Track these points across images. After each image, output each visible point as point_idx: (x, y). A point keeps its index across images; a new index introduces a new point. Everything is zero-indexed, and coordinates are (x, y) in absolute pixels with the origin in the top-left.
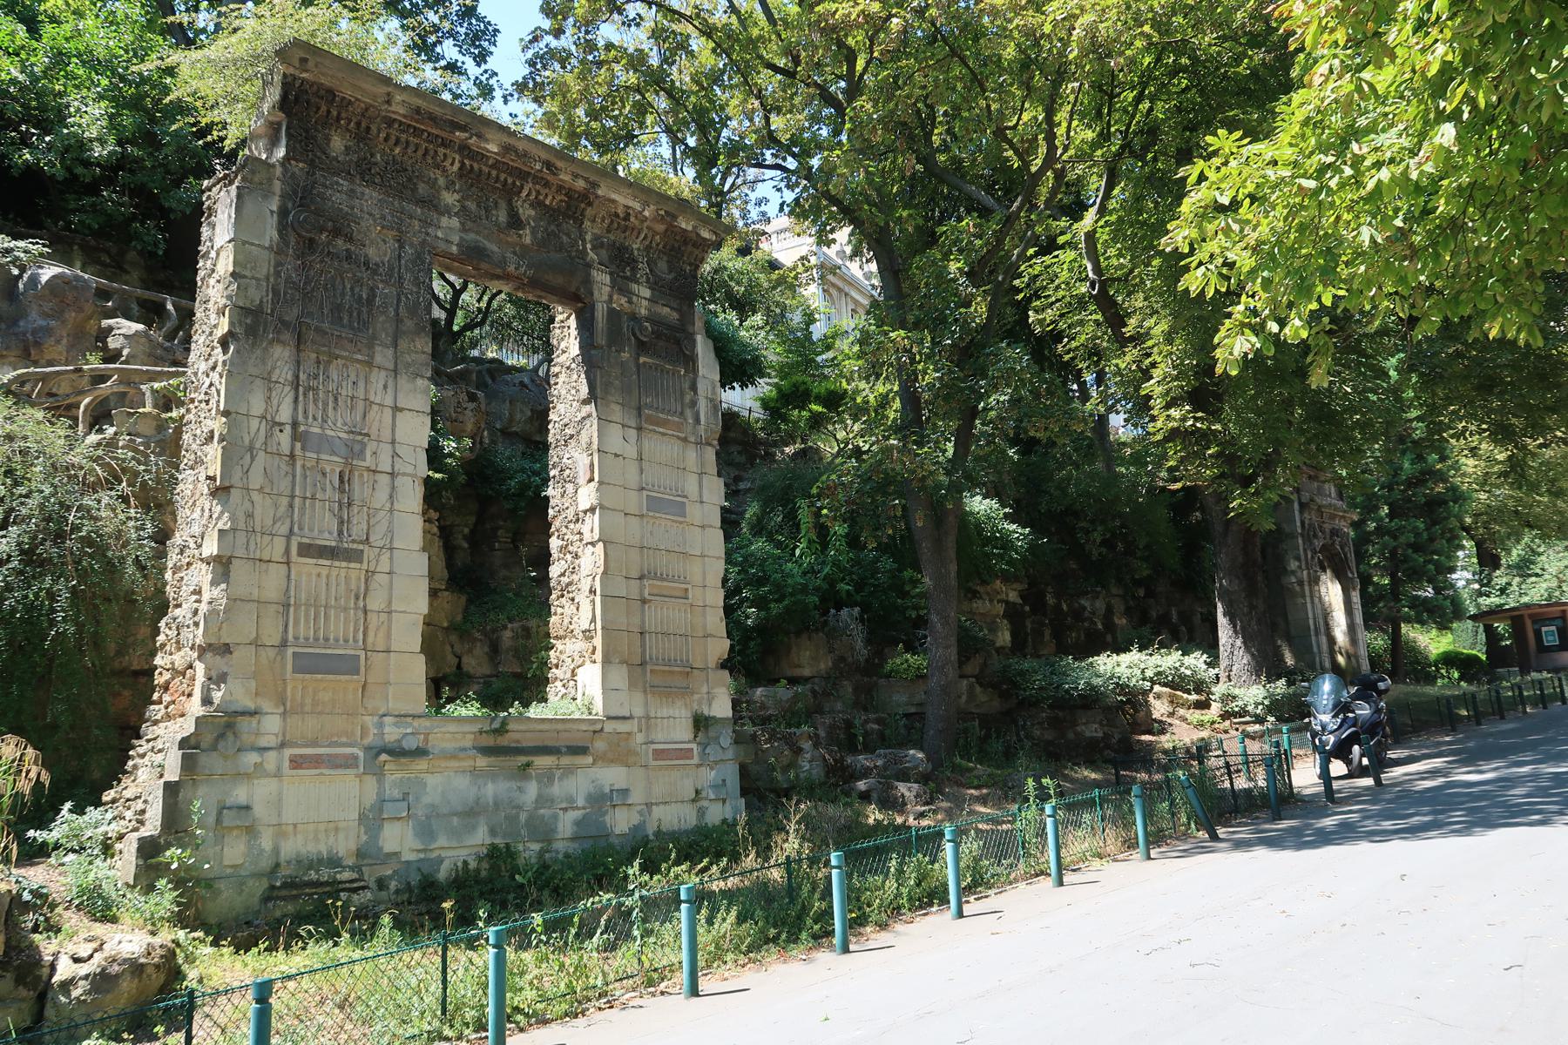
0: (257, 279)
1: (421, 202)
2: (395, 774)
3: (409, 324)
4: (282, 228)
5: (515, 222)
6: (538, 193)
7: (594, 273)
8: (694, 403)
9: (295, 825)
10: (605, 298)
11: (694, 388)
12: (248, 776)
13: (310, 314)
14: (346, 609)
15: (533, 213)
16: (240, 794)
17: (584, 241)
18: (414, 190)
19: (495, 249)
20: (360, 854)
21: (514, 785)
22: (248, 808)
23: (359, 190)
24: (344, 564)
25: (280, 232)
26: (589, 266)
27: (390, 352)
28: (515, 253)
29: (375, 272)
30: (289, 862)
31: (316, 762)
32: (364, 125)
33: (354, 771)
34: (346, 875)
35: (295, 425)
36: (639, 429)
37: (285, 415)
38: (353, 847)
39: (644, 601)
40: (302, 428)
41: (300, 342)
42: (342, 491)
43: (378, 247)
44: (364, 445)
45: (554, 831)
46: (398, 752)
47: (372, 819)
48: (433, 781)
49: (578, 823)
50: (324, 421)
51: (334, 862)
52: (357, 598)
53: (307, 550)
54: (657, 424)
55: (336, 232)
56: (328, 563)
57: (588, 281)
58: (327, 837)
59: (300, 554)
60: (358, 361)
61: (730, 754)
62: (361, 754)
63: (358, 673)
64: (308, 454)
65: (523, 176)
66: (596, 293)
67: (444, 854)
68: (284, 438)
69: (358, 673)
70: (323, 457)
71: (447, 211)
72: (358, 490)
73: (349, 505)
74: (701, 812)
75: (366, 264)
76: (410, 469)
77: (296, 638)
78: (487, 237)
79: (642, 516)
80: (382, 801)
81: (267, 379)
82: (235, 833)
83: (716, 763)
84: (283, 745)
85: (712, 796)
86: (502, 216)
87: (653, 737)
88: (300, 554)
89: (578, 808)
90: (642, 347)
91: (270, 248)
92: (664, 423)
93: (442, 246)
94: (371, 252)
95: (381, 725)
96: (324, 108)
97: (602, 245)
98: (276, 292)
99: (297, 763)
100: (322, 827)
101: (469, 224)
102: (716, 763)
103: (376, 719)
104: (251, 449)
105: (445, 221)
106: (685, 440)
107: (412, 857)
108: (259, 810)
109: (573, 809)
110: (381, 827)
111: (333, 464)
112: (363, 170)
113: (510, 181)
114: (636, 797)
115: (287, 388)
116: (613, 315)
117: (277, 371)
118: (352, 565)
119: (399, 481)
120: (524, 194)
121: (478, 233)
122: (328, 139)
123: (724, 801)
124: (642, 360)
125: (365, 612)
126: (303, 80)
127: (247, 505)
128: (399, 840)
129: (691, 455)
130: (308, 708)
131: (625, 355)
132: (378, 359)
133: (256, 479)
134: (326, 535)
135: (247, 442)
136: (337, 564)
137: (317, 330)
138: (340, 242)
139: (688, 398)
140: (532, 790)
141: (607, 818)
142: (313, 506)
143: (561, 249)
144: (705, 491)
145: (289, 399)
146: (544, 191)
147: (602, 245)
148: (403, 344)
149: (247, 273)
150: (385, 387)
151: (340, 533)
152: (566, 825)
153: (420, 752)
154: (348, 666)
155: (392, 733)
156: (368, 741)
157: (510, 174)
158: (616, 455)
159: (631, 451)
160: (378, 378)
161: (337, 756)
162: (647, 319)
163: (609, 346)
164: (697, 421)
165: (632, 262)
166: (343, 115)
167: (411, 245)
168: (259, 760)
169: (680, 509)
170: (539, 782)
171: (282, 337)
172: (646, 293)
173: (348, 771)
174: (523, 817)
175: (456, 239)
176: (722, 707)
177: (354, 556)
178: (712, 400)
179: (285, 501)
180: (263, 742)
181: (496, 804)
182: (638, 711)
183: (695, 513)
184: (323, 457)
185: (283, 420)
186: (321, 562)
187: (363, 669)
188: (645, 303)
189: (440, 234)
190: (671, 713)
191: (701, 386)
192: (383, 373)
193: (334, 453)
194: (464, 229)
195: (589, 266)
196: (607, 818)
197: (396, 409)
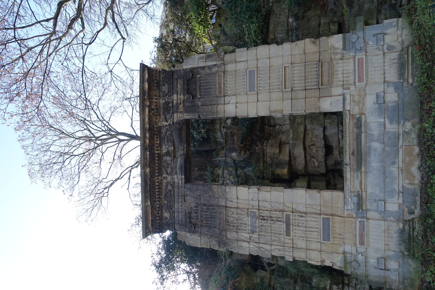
0: (210, 241)
1: (173, 187)
2: (368, 205)
3: (210, 193)
4: (194, 232)
5: (168, 154)
6: (157, 147)
7: (175, 121)
8: (209, 67)
9: (385, 245)
10: (182, 115)
11: (203, 68)
12: (366, 258)
13: (215, 227)
14: (307, 221)
15: (163, 146)
16: (372, 261)
17: (166, 126)
18: (170, 191)
19: (179, 160)
20: (398, 221)
21: (372, 154)
22: (378, 259)
23: (176, 210)
24: (291, 221)
25: (195, 233)
26: (173, 123)
27: (221, 200)
28: (178, 151)
29: (198, 204)
30: (399, 248)
31: (362, 236)
32: (158, 209)
33: (366, 222)
34: (407, 228)
35: (249, 233)
36: (224, 96)
37: (247, 235)
38: (395, 224)
39: (292, 90)
40: (250, 232)
41: (226, 230)
42: (267, 220)
43: (191, 202)
44: (251, 212)
45: (394, 133)
46: (360, 205)
47: (385, 215)
48: (369, 190)
49: (391, 122)
50: (246, 224)
51: (402, 232)
52: (302, 216)
53: (288, 234)
54: (221, 88)
55: (190, 218)
56: (291, 226)
57: (179, 123)
58: (391, 233)
59: (290, 236)
60: (226, 212)
61: (360, 34)
62: (359, 219)
63: (329, 219)
64: (257, 230)
65: (152, 155)
66: (181, 119)
67: (401, 185)
68: (255, 236)
69: (329, 219)
70: (257, 226)
71: (173, 179)
72: (266, 214)
73: (271, 217)
74: (390, 48)
75: (196, 207)
76: (256, 195)
77: (318, 239)
78: (176, 164)
79: (258, 93)
80: (377, 210)
81: (238, 240)
82: (386, 264)
83: (365, 42)
84: (355, 245)
85: (382, 43)
86: (168, 158)
87: (352, 82)
88: (290, 236)
89: (385, 121)
90: (194, 97)
91: (200, 236)
92: (220, 84)
93: (183, 181)
94: (193, 205)
95: (348, 210)
96: (158, 221)
97: (165, 118)
98: (212, 236)
99: (362, 243)
100: (386, 235)
101: (174, 171)
102: (365, 42)
103: (345, 211)
104: (259, 248)
105: (176, 181)
106: (224, 72)
107: (401, 199)
108: (379, 255)
109: (385, 124)
110: (388, 211)
111: (258, 223)
112: (170, 208)
113: (157, 159)
114: (380, 88)
115: (239, 234)
116: (187, 110)
117: (235, 236)
118: (291, 218)
119: (260, 199)
120: (159, 152)
121: (176, 168)
122: (166, 218)
123: (385, 34)
124: (199, 97)
125: (306, 213)
126: (152, 229)
127: (276, 250)
128: (393, 206)
129: (230, 67)
130: (342, 237)
131: (200, 104)
132: (223, 204)
133: (268, 247)
134: (282, 226)
135: (257, 249)
136: (291, 223)
137: (219, 225)
138: (192, 216)
139: (208, 71)
140: (376, 145)
141: (390, 105)
142: (274, 230)
143: (172, 135)
144: (243, 59)
145: (242, 234)
146: (156, 145)
147: (165, 118)
148: (217, 196)
149: (209, 244)
150: (231, 201)
151: (281, 221)
152: (391, 128)
153: (360, 197)
154: (326, 222)
155: (351, 206)
156: (354, 215)
157: (154, 159)
158: (236, 107)
159: (233, 100)
160: (229, 204)
161: (360, 228)
162: (184, 96)
163: (198, 112)
164: (215, 65)
165: (167, 103)
166: (157, 215)
167: (187, 192)
168: (361, 254)
169: (252, 73)
170: (372, 141)
171: (224, 234)
172: (175, 96)
173: (366, 225)
174: (387, 149)
175: (180, 176)
176: (336, 41)
177: (288, 217)
178: (206, 59)
179: (273, 238)
180: (354, 252)
181: (381, 162)
182: (340, 90)
183: (252, 64)
184: (257, 226)
185: (249, 236)
186: (291, 229)
187: (327, 217)
188: (179, 97)
189: (180, 182)
190: (340, 72)
191: (202, 64)
192: (227, 202)
193: (256, 222)
194: (176, 173)
195: (173, 123)
196: (390, 105)
197: (237, 198)
